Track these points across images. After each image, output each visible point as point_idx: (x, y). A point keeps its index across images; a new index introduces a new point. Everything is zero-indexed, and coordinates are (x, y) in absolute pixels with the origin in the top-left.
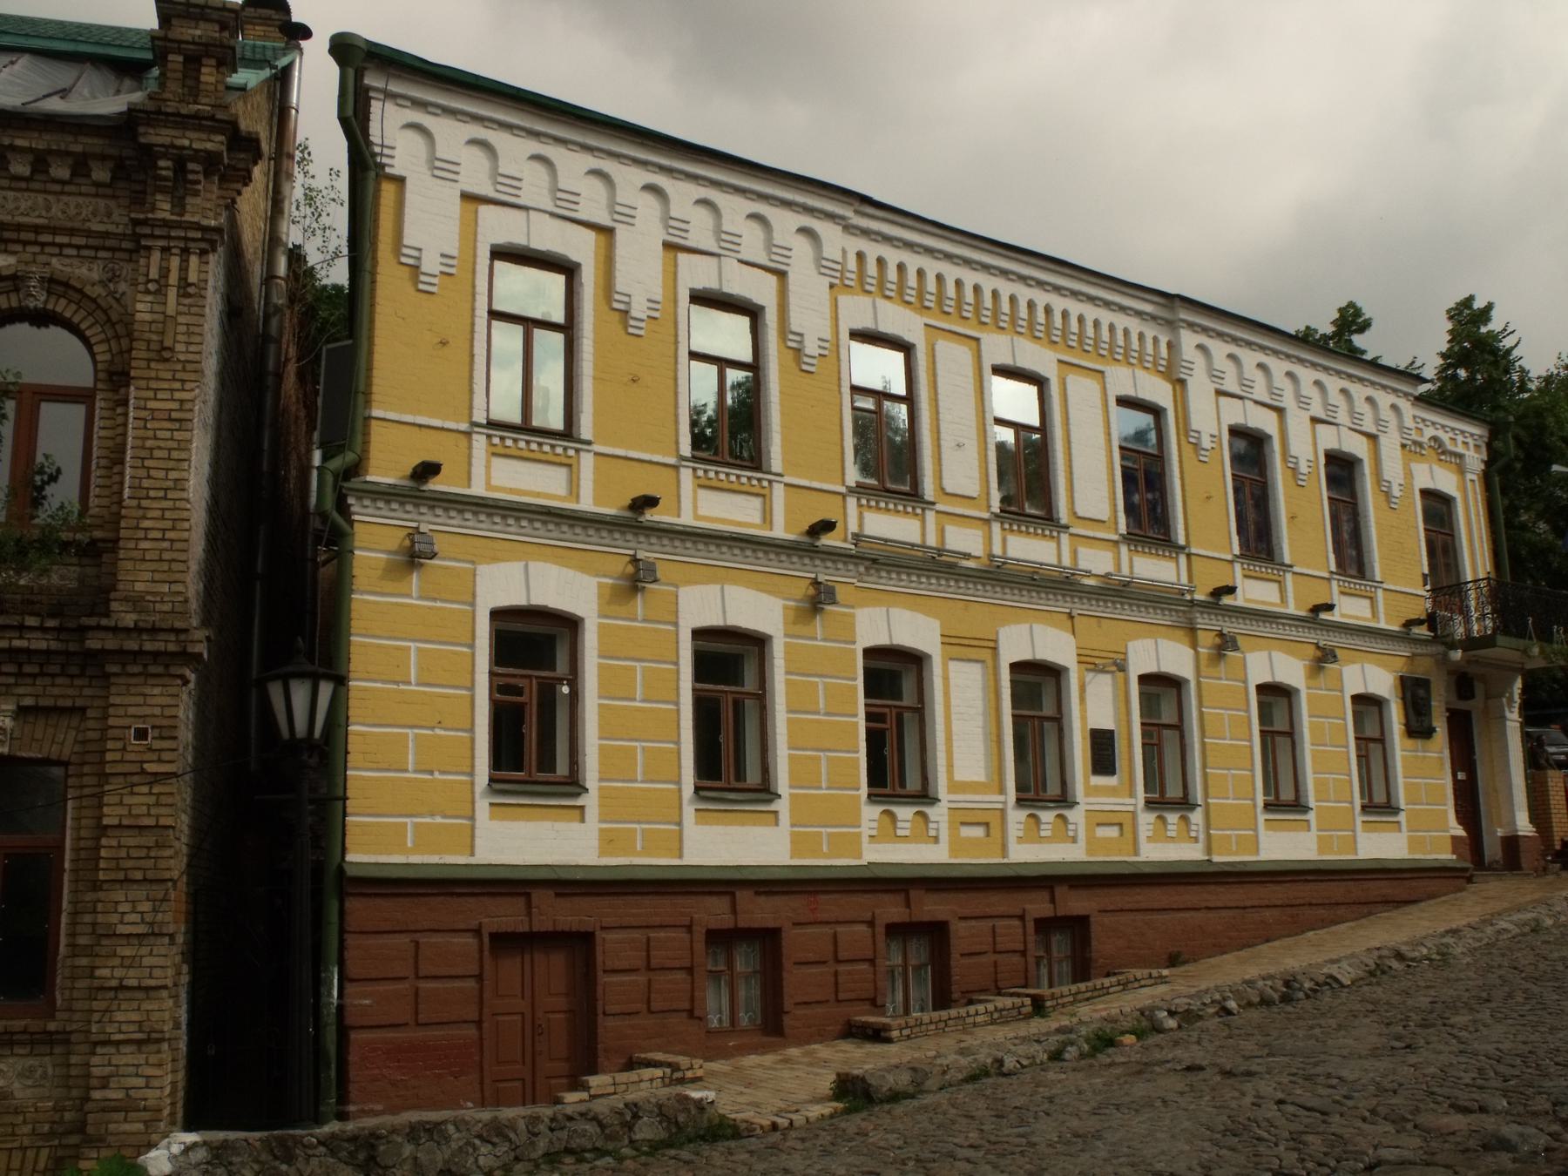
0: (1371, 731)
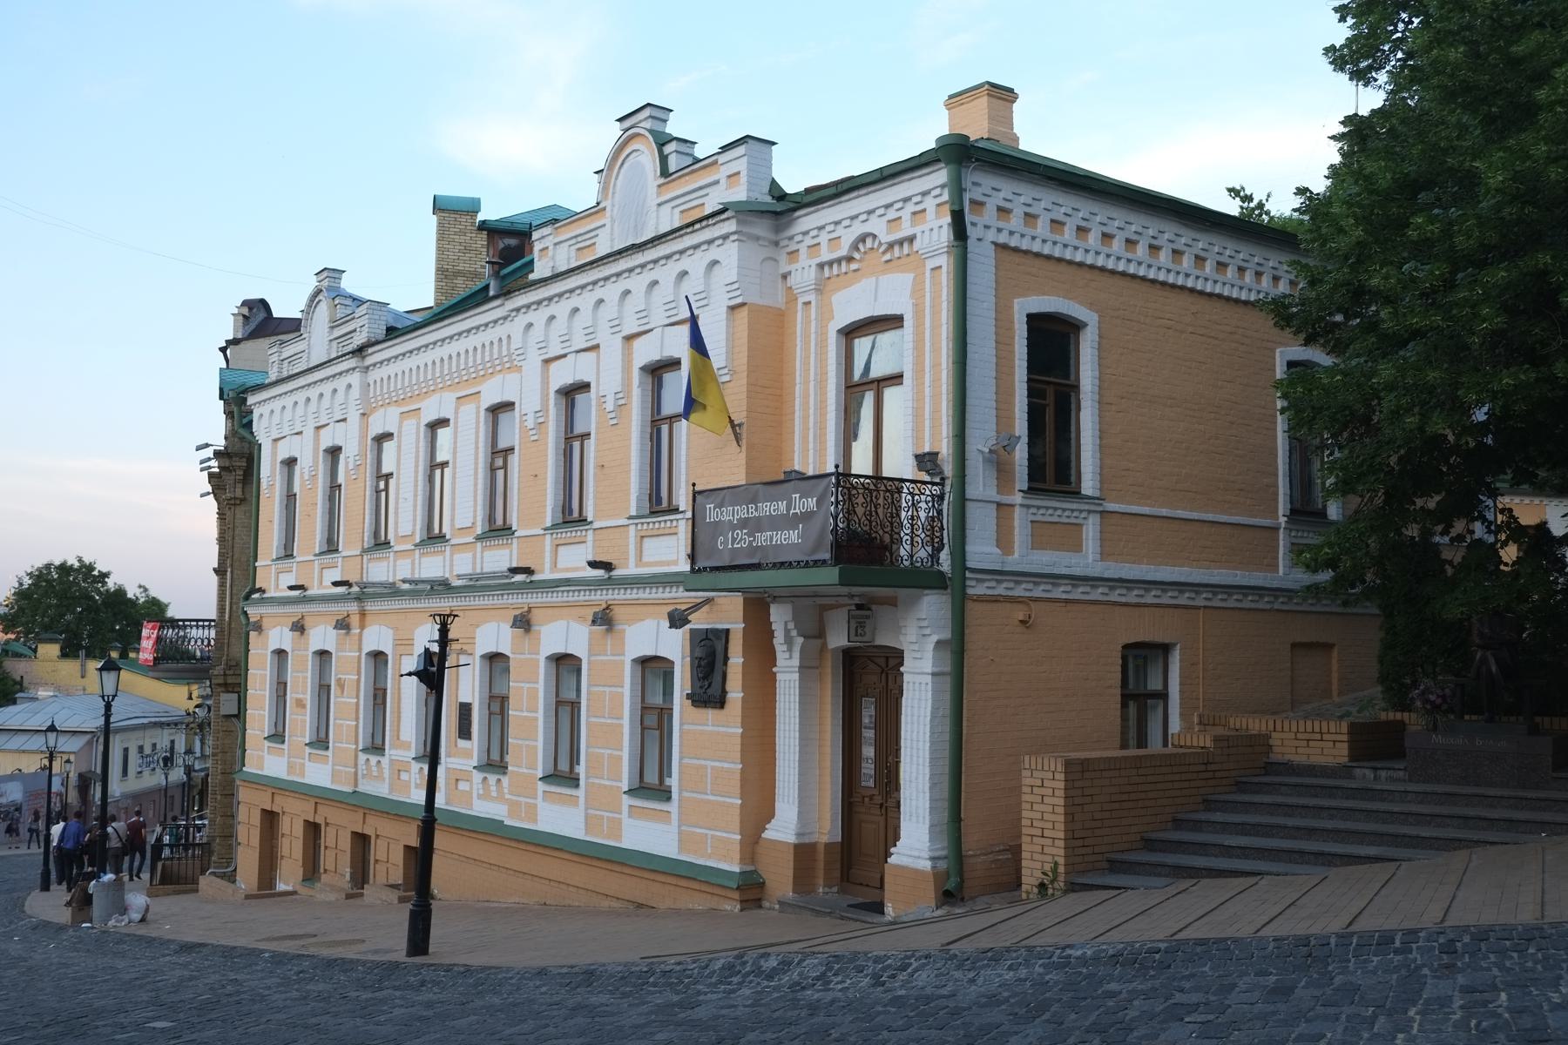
0: (657, 700)
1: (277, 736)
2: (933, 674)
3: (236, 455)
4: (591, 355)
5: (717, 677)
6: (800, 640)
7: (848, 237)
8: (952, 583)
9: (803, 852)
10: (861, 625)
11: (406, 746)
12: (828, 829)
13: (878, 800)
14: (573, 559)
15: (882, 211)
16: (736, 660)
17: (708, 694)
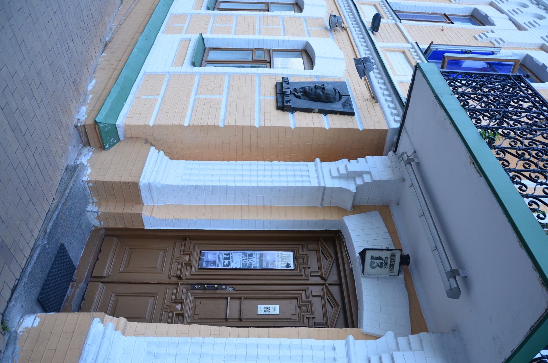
6: (353, 189)
9: (131, 192)
12: (156, 216)
13: (186, 273)
17: (288, 97)
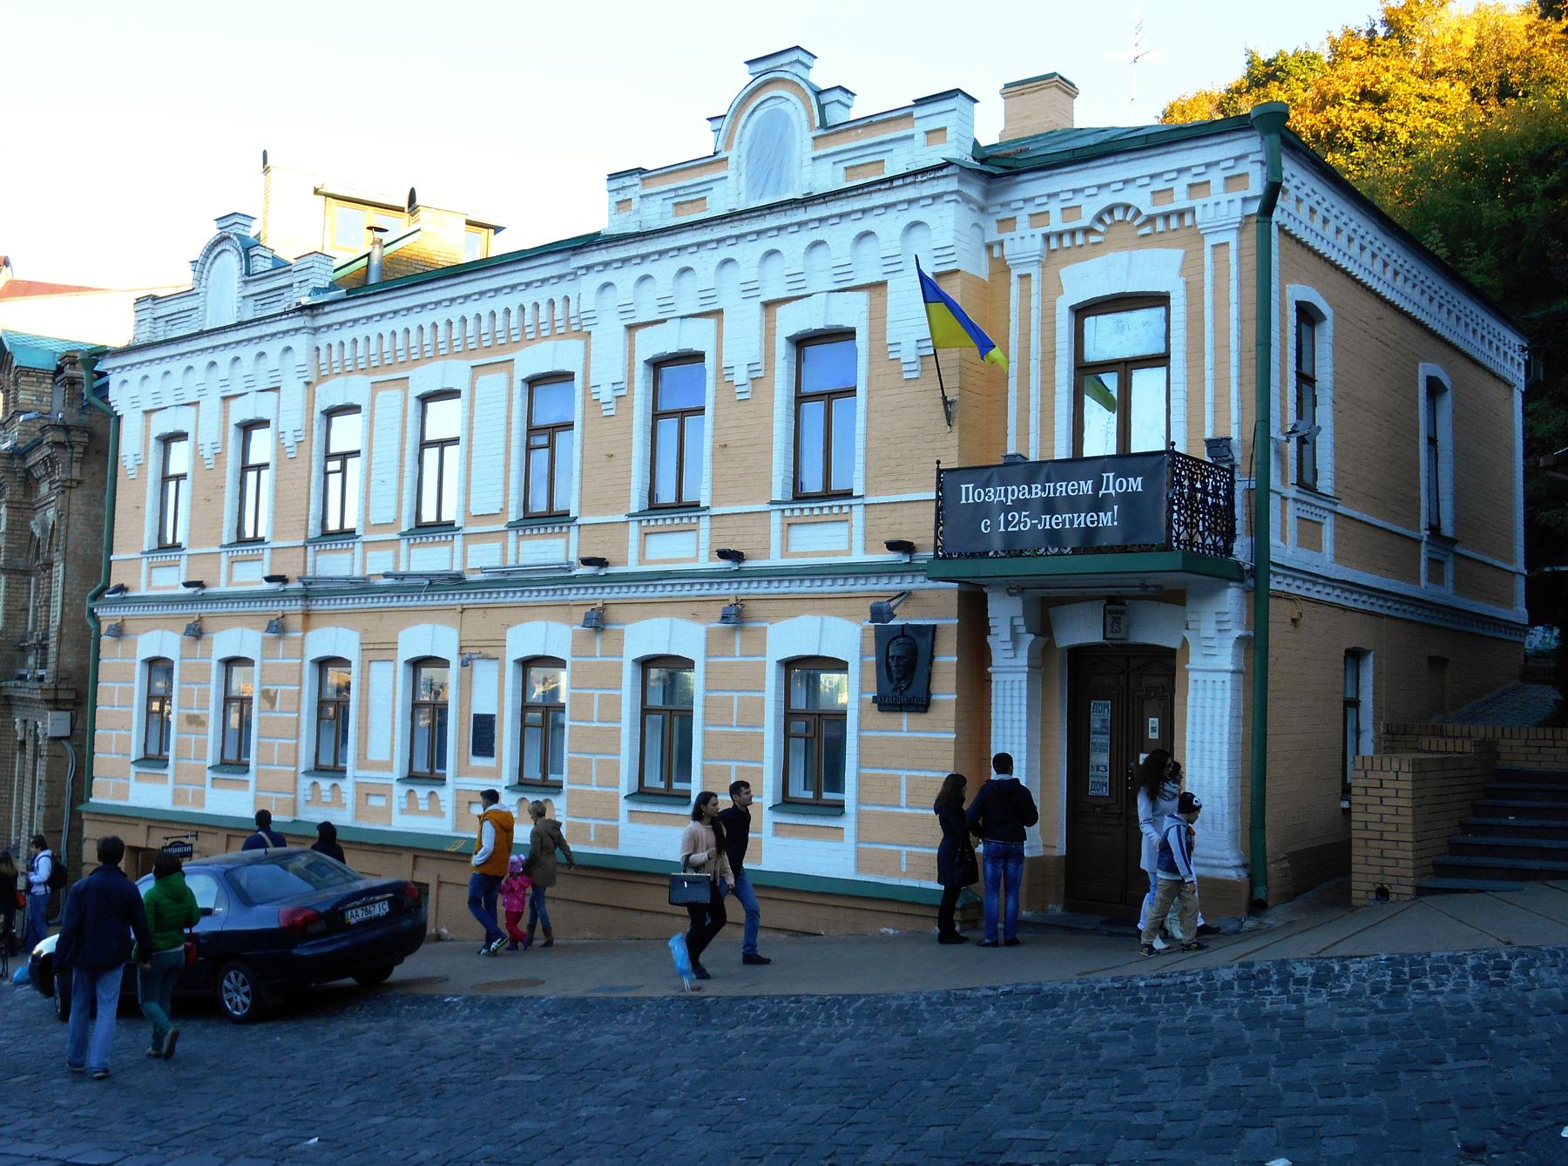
1: (154, 760)
2: (1233, 672)
3: (77, 428)
4: (711, 323)
5: (919, 678)
7: (1090, 209)
8: (1255, 579)
10: (1117, 621)
11: (387, 766)
14: (685, 548)
15: (1147, 181)
16: (947, 659)
